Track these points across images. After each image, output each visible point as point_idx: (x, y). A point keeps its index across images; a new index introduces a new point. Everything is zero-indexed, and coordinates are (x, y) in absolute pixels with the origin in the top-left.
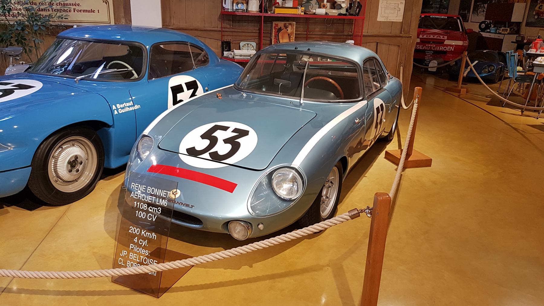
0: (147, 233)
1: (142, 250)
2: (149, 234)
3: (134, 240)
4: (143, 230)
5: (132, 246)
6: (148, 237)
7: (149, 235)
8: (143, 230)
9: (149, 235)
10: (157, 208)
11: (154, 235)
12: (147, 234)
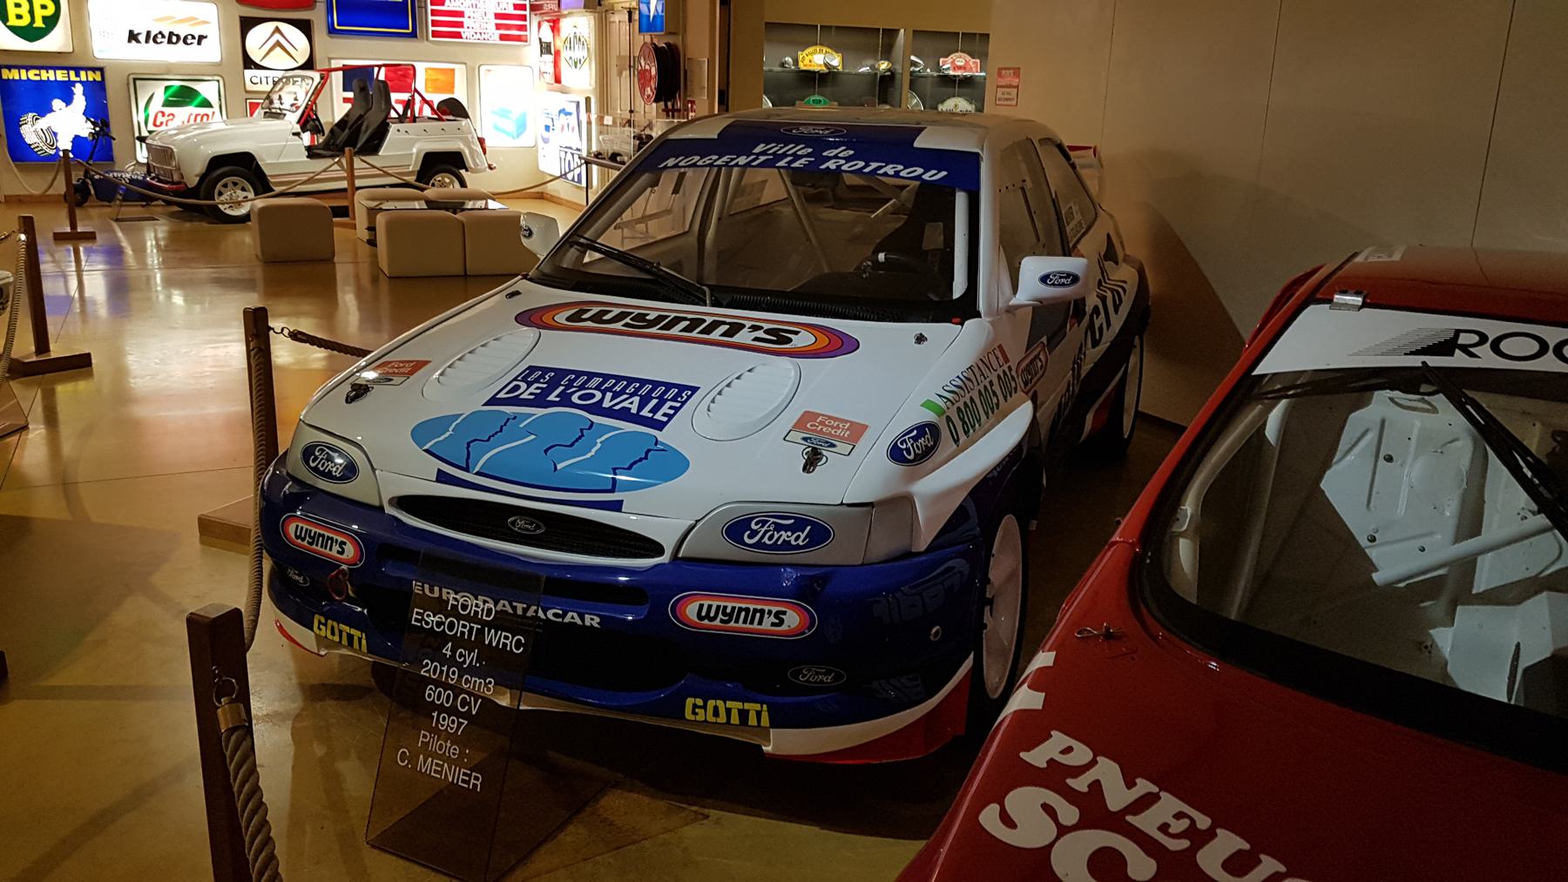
1: (450, 748)
3: (444, 651)
5: (425, 736)
6: (458, 769)
10: (485, 681)
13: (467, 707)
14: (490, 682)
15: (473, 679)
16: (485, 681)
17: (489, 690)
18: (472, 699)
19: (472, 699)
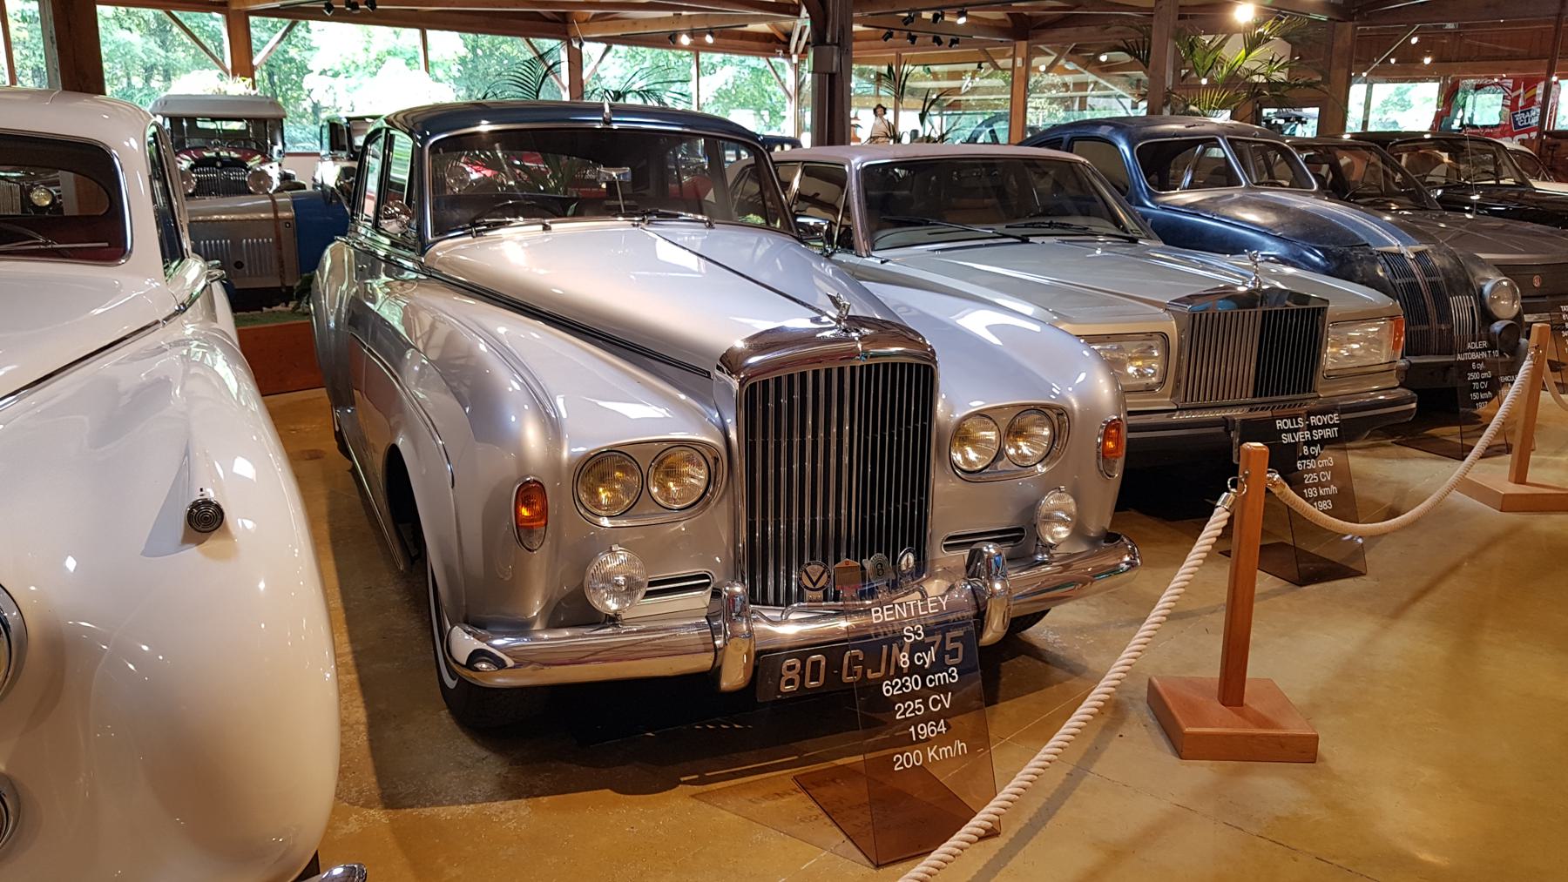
0: (941, 750)
2: (946, 749)
4: (929, 749)
7: (948, 750)
8: (929, 749)
9: (948, 750)
11: (959, 746)
12: (943, 751)
13: (940, 705)
14: (953, 671)
15: (936, 676)
16: (947, 672)
17: (954, 678)
18: (942, 695)
19: (942, 695)
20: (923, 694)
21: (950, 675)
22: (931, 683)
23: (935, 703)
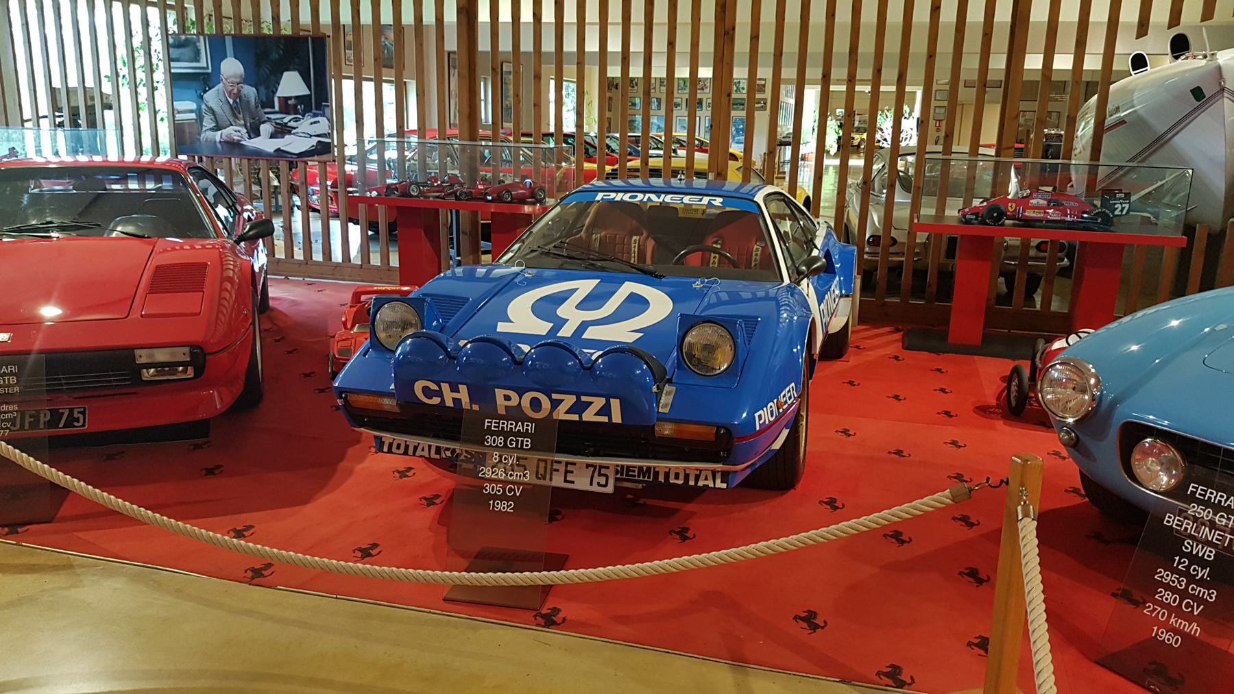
13: (1190, 609)
15: (1199, 588)
17: (1211, 598)
18: (1195, 604)
19: (1195, 604)
20: (1184, 594)
21: (1209, 594)
22: (1192, 590)
23: (1188, 605)
